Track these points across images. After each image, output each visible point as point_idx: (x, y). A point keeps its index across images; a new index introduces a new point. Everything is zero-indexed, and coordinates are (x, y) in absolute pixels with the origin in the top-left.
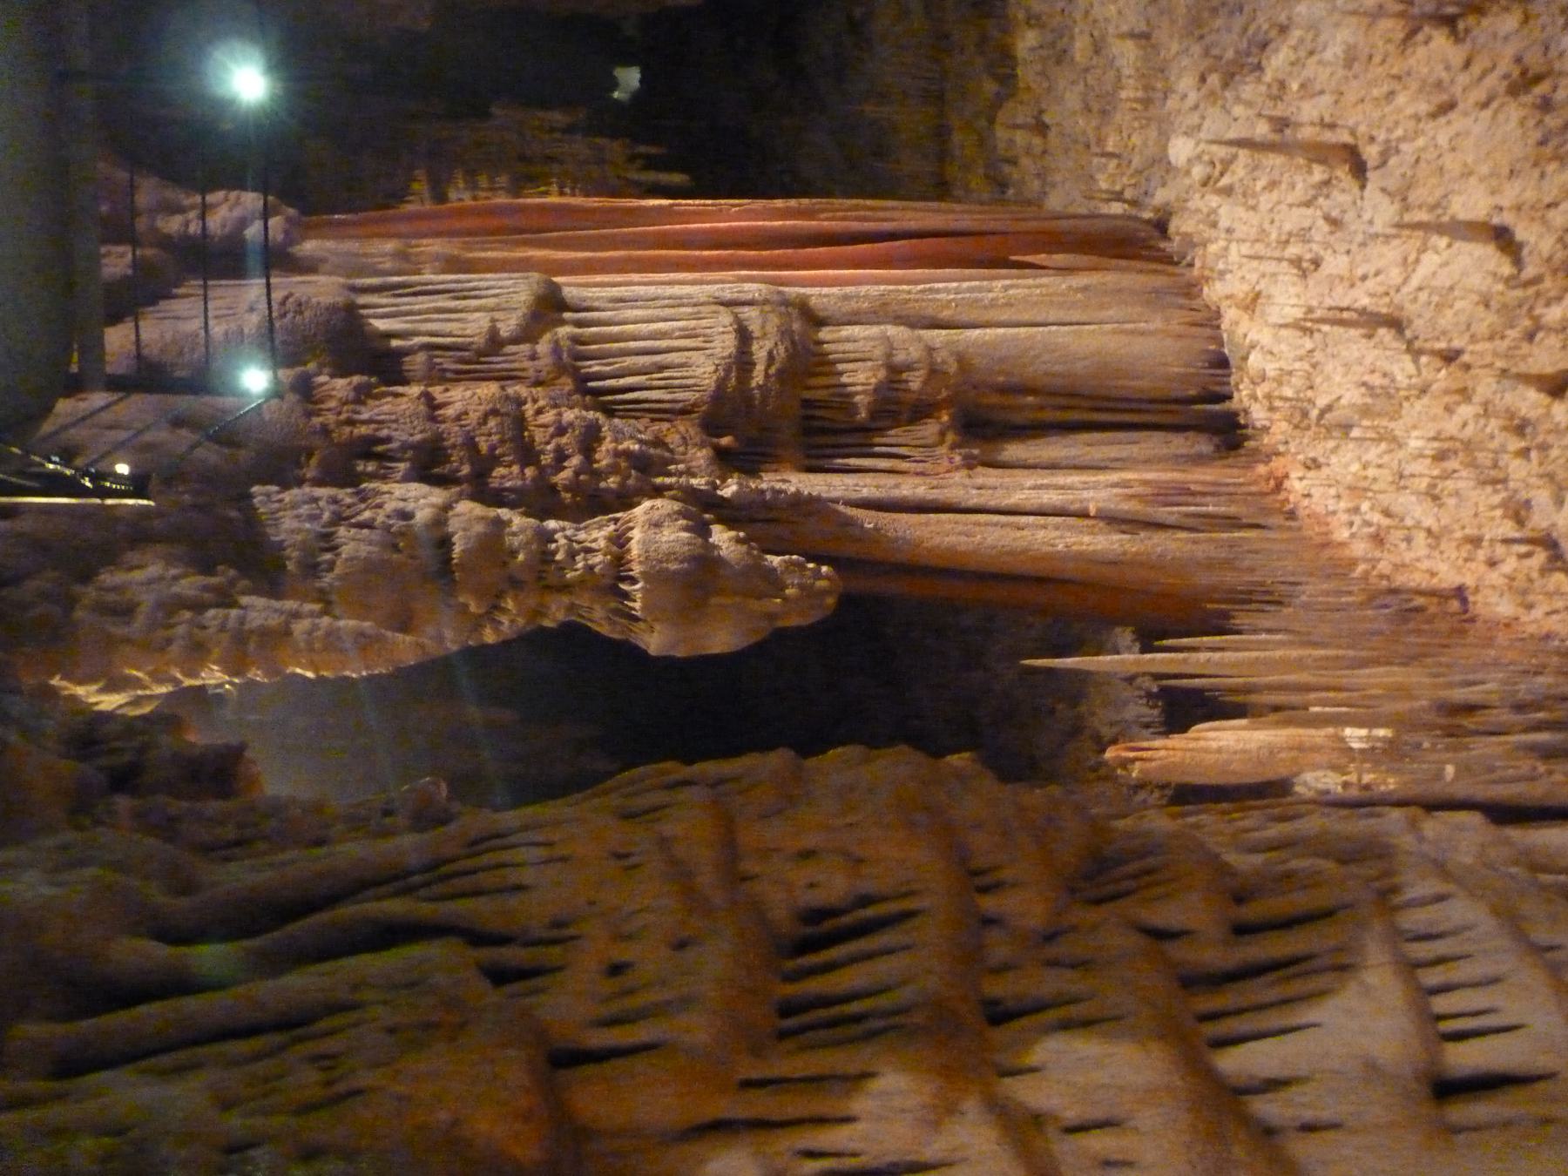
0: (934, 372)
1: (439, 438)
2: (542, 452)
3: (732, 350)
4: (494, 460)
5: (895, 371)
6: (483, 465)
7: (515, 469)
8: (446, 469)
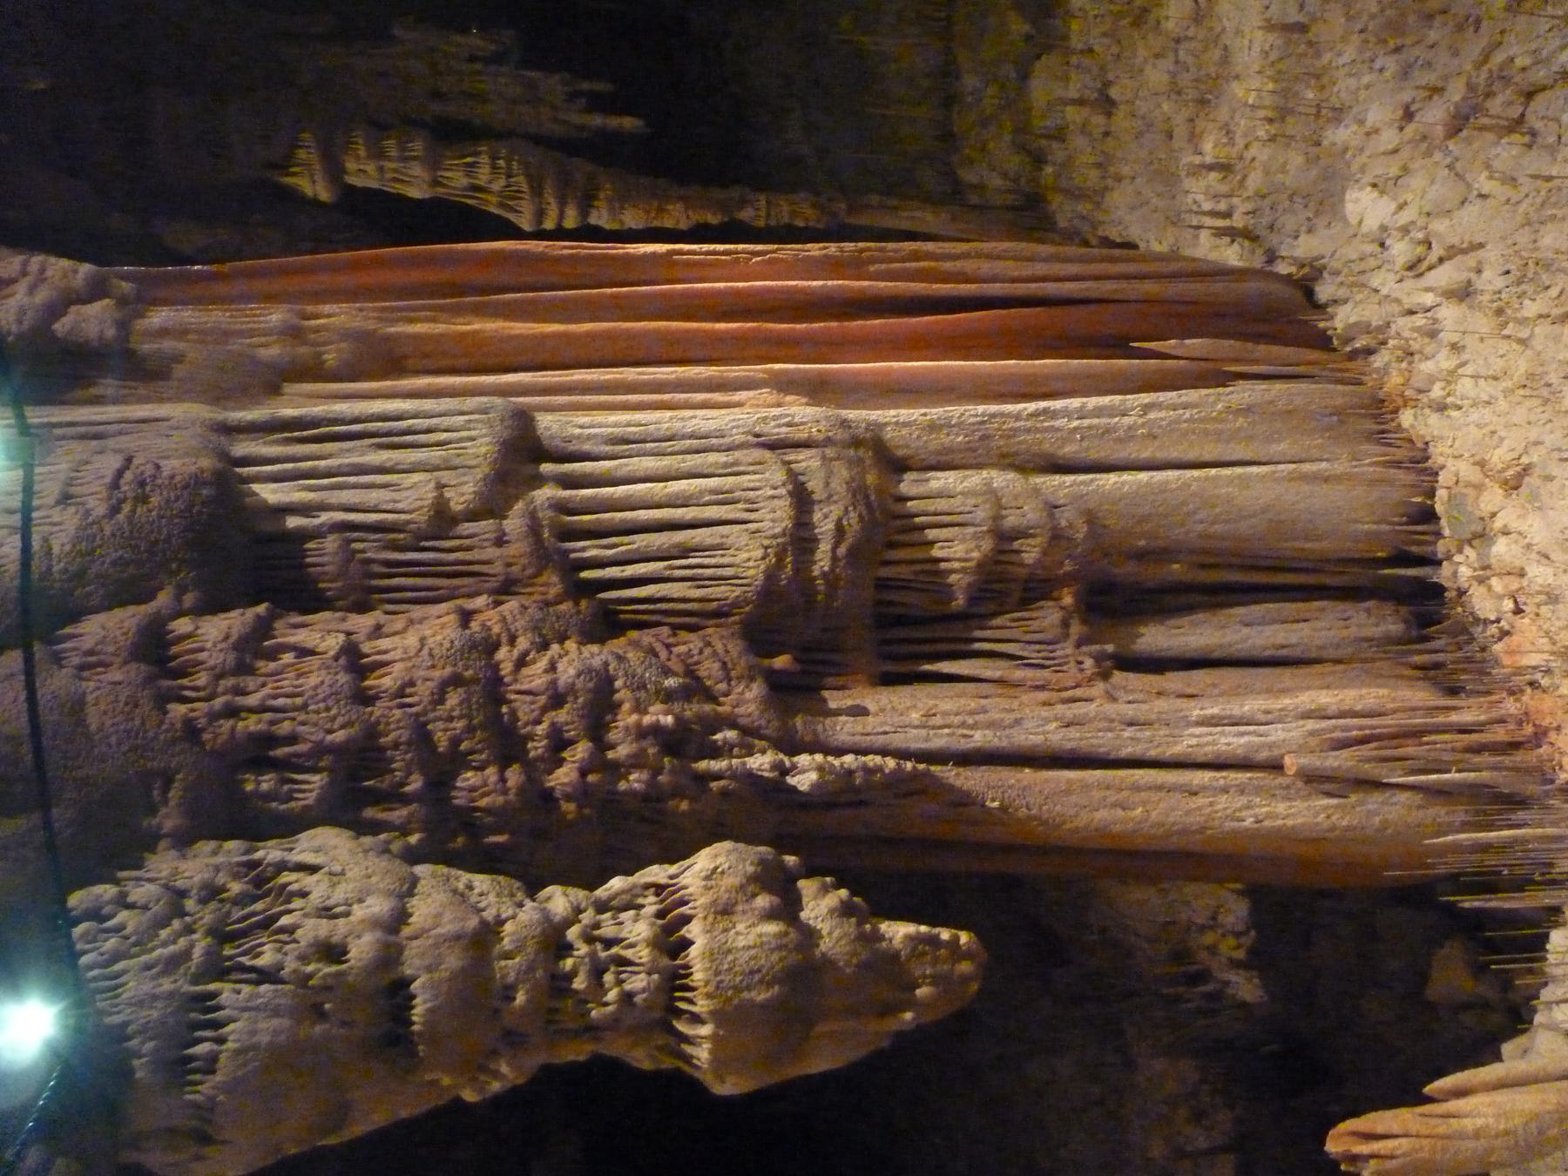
1: (372, 732)
2: (531, 737)
3: (788, 523)
4: (457, 761)
5: (1005, 538)
6: (443, 770)
7: (491, 773)
8: (385, 783)
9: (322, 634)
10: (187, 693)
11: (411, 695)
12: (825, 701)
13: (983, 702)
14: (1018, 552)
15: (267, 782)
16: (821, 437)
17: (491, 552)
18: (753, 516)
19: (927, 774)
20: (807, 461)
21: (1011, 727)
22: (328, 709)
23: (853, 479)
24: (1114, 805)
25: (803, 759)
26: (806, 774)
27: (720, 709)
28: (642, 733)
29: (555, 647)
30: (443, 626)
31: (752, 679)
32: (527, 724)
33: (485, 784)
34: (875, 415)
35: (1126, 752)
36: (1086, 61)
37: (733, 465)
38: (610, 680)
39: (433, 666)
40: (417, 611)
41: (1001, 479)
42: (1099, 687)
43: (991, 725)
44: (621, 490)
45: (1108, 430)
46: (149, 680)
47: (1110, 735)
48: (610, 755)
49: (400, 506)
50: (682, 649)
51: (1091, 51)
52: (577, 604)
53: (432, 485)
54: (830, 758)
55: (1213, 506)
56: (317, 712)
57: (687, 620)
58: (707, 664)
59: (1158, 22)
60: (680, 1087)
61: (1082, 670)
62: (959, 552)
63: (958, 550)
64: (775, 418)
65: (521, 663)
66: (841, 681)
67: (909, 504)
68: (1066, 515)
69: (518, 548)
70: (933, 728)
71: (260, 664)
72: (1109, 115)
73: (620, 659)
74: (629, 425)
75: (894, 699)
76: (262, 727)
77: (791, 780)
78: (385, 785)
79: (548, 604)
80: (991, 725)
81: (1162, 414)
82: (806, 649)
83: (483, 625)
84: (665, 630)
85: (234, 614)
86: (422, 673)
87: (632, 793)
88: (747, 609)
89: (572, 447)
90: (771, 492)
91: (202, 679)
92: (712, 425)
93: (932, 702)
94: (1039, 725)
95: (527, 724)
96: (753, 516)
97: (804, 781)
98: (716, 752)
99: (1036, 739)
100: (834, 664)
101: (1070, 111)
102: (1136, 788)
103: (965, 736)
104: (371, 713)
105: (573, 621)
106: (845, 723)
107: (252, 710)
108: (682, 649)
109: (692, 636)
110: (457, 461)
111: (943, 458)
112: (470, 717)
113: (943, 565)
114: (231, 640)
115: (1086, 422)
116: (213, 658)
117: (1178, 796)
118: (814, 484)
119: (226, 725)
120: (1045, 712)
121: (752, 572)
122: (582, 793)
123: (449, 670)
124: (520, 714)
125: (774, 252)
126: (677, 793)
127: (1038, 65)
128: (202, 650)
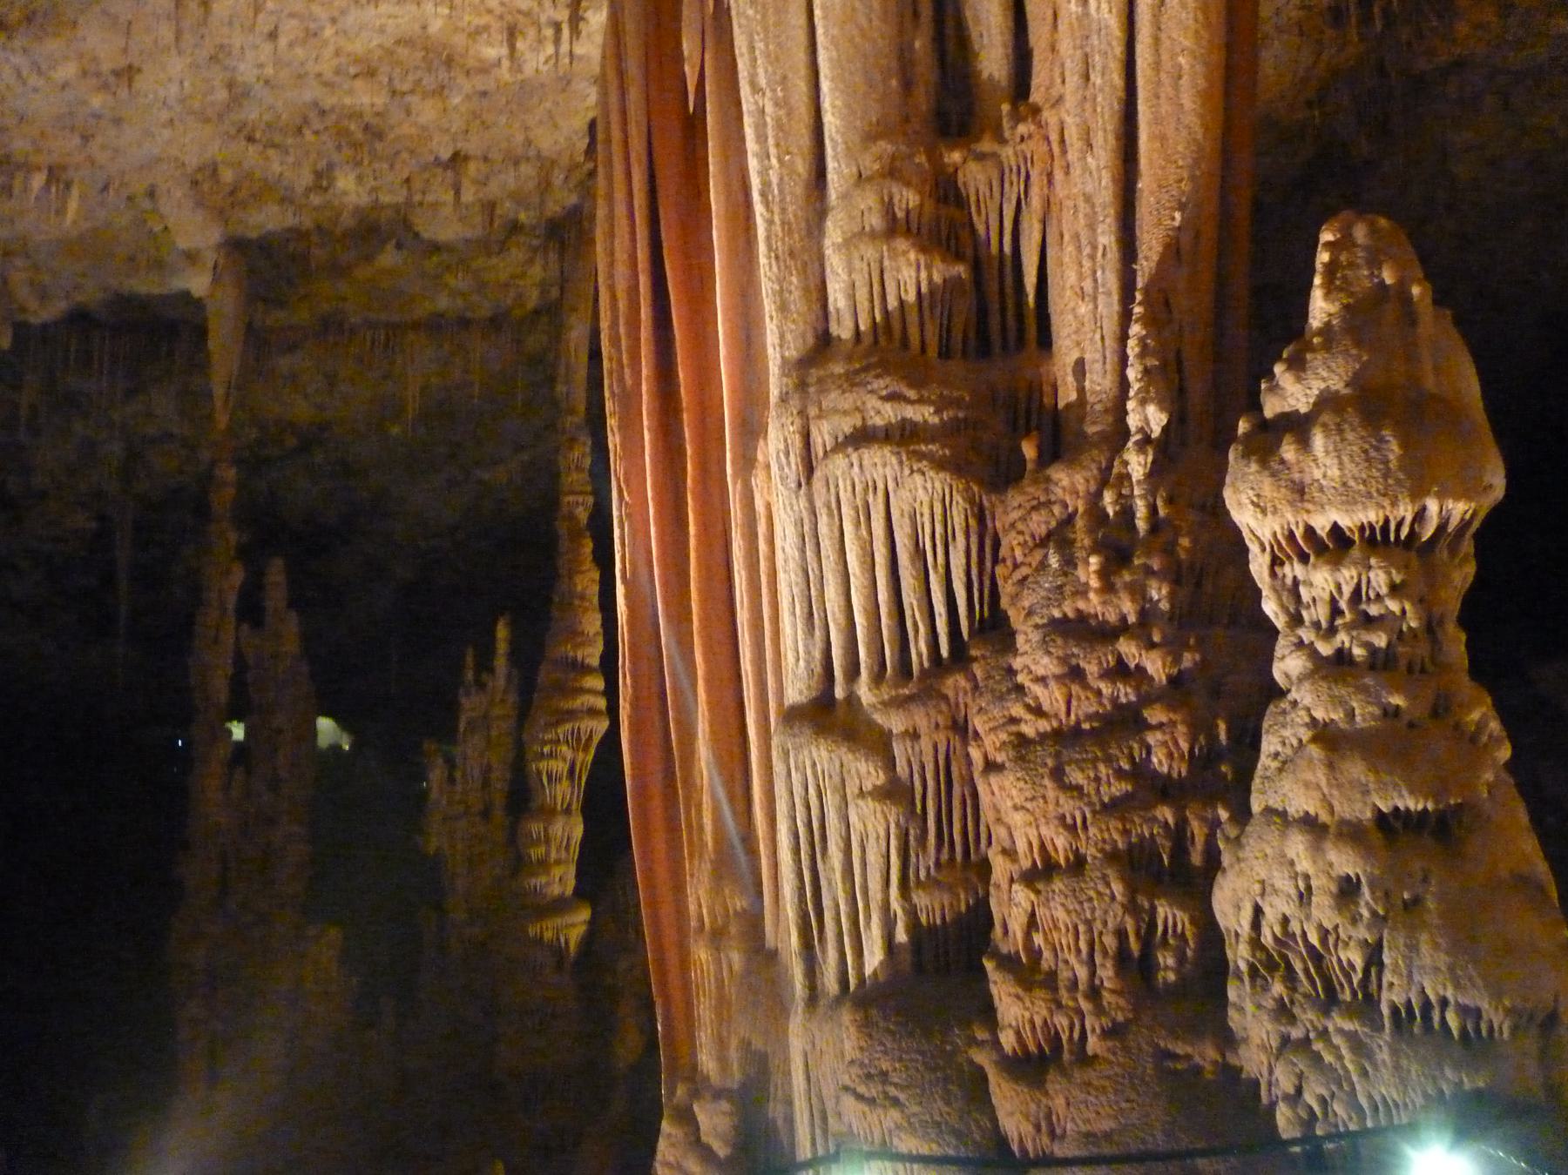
0: (892, 171)
1: (1112, 857)
2: (1114, 700)
3: (887, 450)
4: (1140, 773)
5: (895, 227)
6: (1151, 787)
7: (1153, 738)
8: (1165, 847)
9: (1012, 907)
10: (1076, 1035)
11: (1074, 819)
12: (1068, 406)
13: (1067, 238)
14: (908, 212)
15: (1166, 959)
16: (798, 421)
17: (925, 744)
18: (881, 486)
19: (1147, 291)
20: (823, 434)
21: (1093, 206)
22: (1090, 899)
23: (840, 387)
24: (1176, 88)
25: (1133, 421)
26: (1148, 417)
27: (1081, 510)
28: (1108, 588)
29: (1020, 678)
30: (1002, 788)
31: (1048, 480)
32: (1101, 704)
33: (1165, 744)
34: (774, 368)
35: (1118, 80)
36: (417, 184)
37: (829, 508)
38: (1053, 622)
39: (1044, 797)
40: (987, 815)
41: (834, 233)
42: (1048, 116)
43: (1092, 227)
44: (860, 620)
45: (779, 126)
46: (1064, 1072)
47: (1099, 99)
48: (1132, 619)
49: (882, 833)
50: (1018, 553)
51: (408, 180)
52: (975, 659)
53: (861, 802)
54: (1132, 393)
55: (854, 9)
56: (1093, 910)
57: (988, 549)
58: (1033, 526)
59: (378, 114)
60: (1493, 534)
61: (1030, 136)
62: (911, 274)
63: (908, 274)
64: (781, 468)
65: (1038, 711)
66: (1047, 389)
67: (862, 328)
68: (867, 163)
69: (921, 718)
70: (1096, 288)
71: (1045, 965)
72: (467, 158)
73: (1030, 613)
74: (794, 614)
75: (1065, 332)
76: (1109, 964)
77: (1156, 431)
78: (1168, 844)
79: (976, 687)
80: (1092, 227)
81: (761, 71)
82: (1015, 430)
83: (999, 750)
84: (999, 570)
85: (994, 990)
86: (1051, 807)
87: (1172, 596)
88: (975, 489)
89: (818, 669)
90: (856, 469)
91: (1061, 1021)
92: (791, 531)
93: (1068, 293)
94: (1092, 176)
95: (1101, 704)
96: (881, 486)
97: (1156, 419)
98: (1127, 513)
99: (1106, 178)
100: (1030, 399)
101: (468, 196)
102: (1157, 66)
103: (1104, 255)
104: (1095, 858)
105: (992, 662)
106: (1092, 382)
107: (1093, 973)
108: (1018, 553)
109: (1004, 542)
110: (837, 779)
111: (815, 296)
112: (1095, 761)
113: (924, 289)
114: (1020, 991)
115: (773, 151)
116: (1040, 1011)
117: (1164, 18)
118: (847, 425)
119: (1107, 997)
120: (1076, 171)
121: (938, 485)
122: (1173, 648)
123: (1047, 782)
124: (1092, 710)
125: (618, 480)
126: (1169, 550)
127: (426, 235)
128: (1032, 1022)
